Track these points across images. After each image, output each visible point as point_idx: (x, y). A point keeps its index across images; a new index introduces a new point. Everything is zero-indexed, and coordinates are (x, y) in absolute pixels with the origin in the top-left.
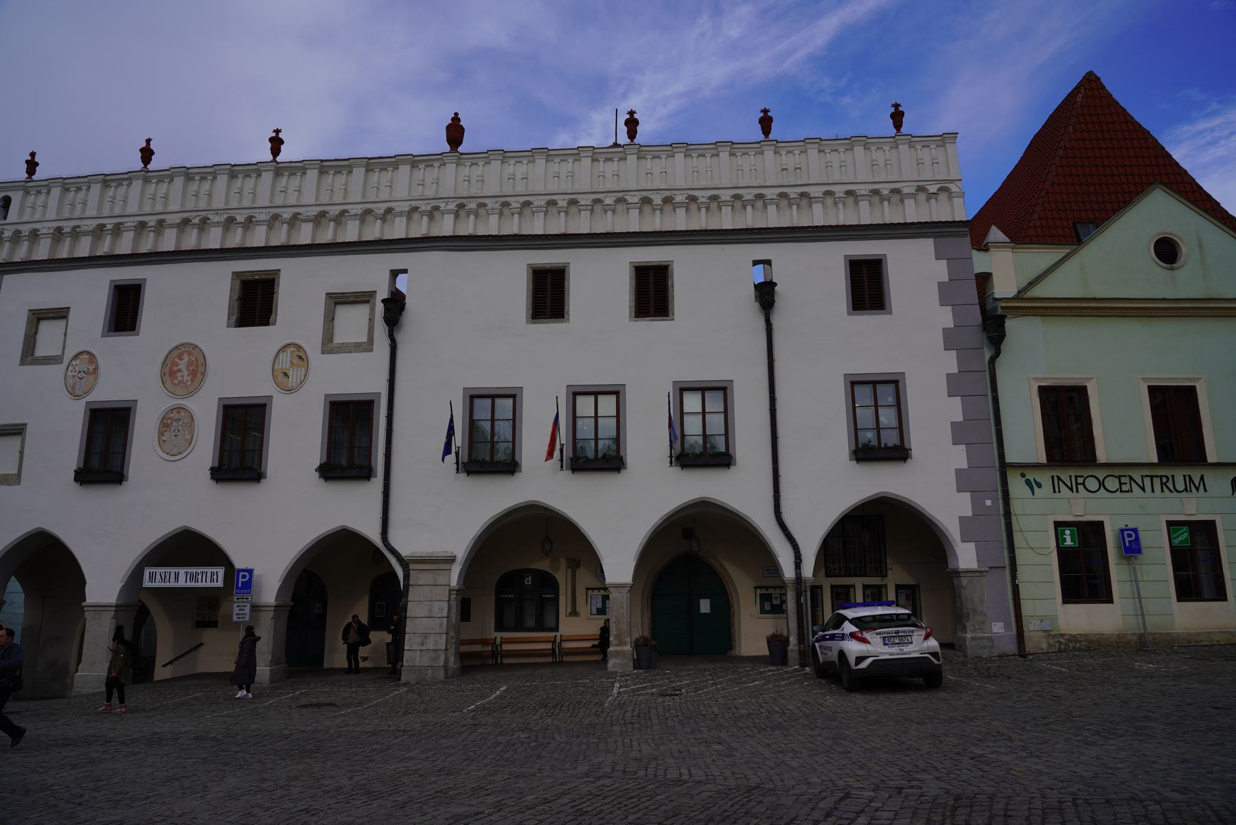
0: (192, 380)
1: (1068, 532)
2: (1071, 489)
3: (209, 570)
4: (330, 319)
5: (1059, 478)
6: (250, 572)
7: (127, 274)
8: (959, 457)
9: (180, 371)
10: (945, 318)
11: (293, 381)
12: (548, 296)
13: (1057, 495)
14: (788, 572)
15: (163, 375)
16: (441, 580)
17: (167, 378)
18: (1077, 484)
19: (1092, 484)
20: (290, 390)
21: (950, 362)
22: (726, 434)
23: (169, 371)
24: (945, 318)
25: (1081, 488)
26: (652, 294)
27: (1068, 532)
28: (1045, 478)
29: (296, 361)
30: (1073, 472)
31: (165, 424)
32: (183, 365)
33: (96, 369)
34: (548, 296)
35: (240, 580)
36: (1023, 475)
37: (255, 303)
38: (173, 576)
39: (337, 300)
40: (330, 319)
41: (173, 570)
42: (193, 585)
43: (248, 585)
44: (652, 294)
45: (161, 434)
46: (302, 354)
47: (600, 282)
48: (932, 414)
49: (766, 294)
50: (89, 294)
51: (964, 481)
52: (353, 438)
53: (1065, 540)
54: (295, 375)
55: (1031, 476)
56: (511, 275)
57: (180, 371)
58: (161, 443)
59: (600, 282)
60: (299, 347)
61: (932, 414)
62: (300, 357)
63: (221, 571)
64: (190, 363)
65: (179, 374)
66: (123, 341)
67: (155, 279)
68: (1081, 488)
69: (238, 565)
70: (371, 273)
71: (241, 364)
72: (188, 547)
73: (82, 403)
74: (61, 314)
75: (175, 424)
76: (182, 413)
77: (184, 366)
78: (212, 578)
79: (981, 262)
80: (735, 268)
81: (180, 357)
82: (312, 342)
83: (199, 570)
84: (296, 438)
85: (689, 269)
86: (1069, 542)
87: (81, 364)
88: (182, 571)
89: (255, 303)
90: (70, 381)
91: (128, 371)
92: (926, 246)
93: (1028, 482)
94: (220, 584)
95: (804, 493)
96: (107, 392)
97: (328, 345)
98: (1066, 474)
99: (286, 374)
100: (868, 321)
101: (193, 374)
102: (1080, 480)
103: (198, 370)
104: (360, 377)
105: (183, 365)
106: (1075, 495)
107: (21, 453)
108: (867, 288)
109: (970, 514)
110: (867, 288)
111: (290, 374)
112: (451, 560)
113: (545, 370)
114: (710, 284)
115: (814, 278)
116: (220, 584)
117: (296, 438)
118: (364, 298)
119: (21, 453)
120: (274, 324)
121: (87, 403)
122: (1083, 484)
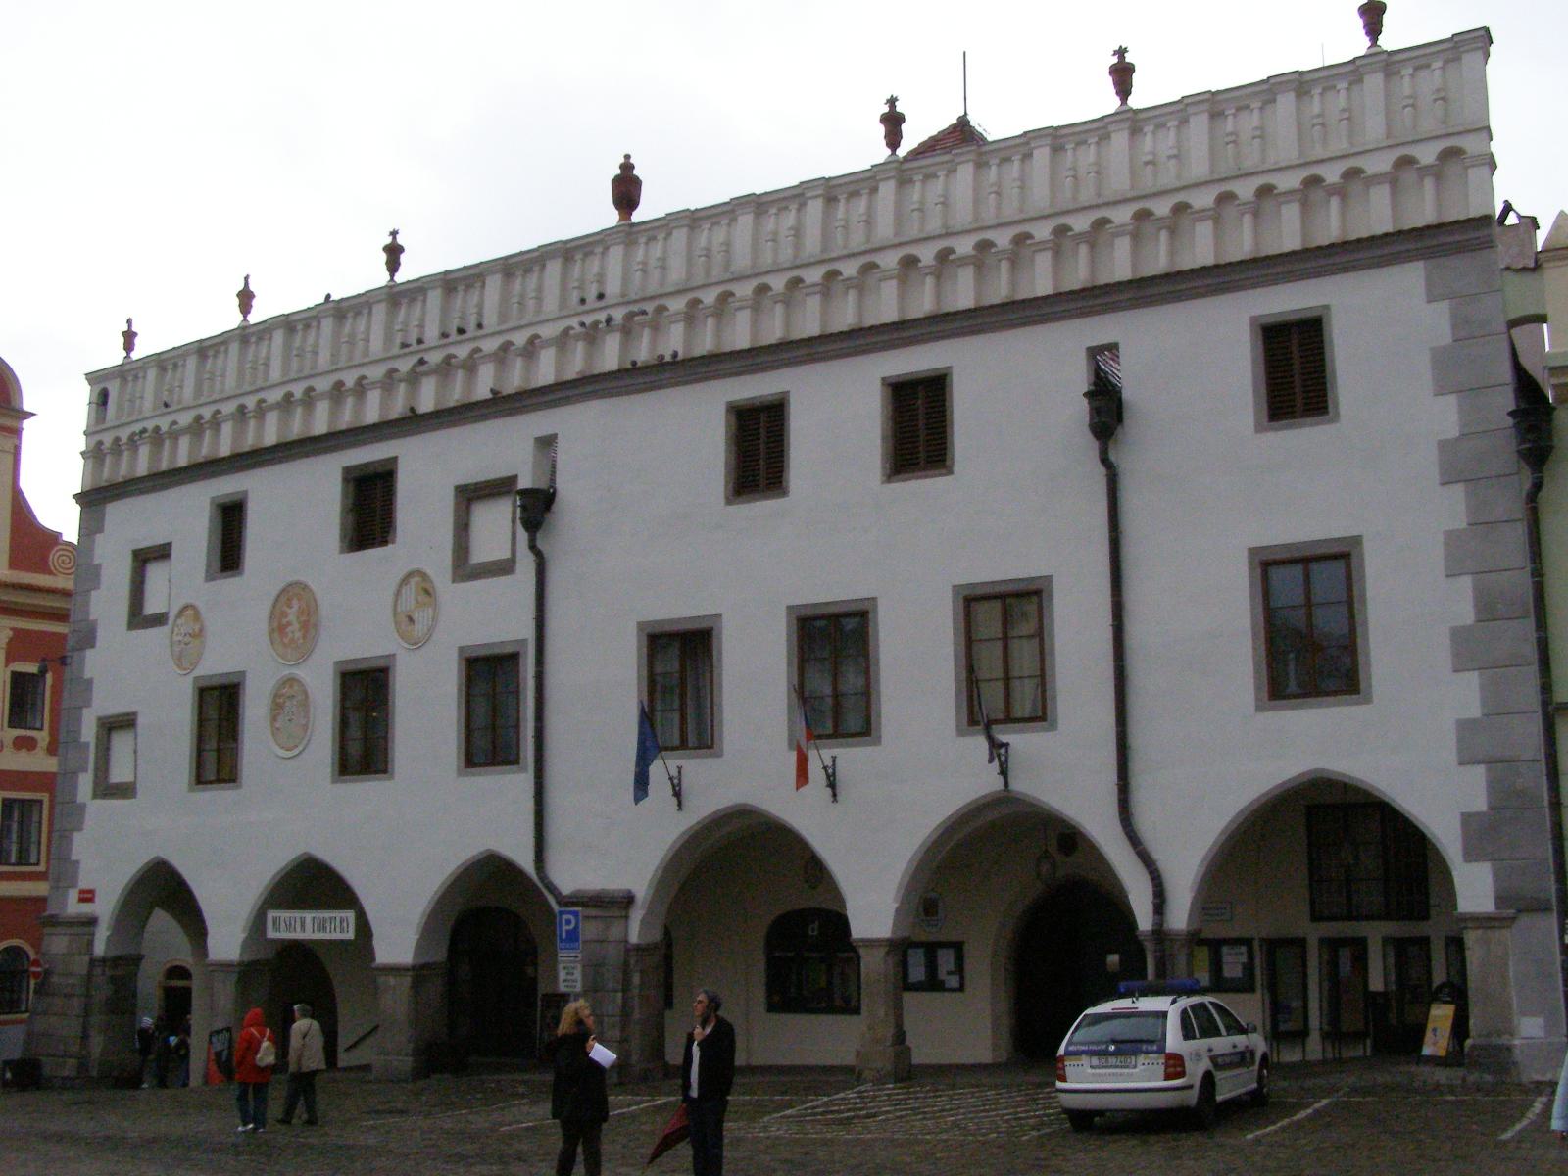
0: (304, 637)
4: (462, 528)
7: (226, 486)
8: (1465, 696)
9: (289, 624)
10: (1445, 417)
11: (419, 629)
12: (758, 454)
14: (1144, 921)
15: (271, 632)
16: (615, 932)
17: (276, 635)
21: (1451, 508)
22: (1042, 676)
23: (278, 628)
24: (1445, 417)
26: (919, 429)
29: (422, 597)
31: (277, 706)
34: (758, 454)
37: (370, 512)
38: (298, 920)
39: (470, 495)
40: (462, 528)
41: (297, 914)
44: (919, 429)
45: (274, 719)
46: (428, 586)
47: (836, 417)
48: (1415, 610)
49: (1107, 408)
51: (1473, 743)
54: (422, 617)
57: (289, 624)
58: (276, 731)
59: (836, 417)
61: (1415, 610)
62: (427, 592)
63: (350, 915)
65: (289, 629)
66: (230, 585)
70: (502, 449)
71: (360, 607)
72: (312, 883)
73: (190, 679)
74: (162, 552)
76: (296, 688)
77: (295, 615)
78: (337, 926)
80: (1047, 367)
82: (438, 562)
83: (327, 914)
84: (427, 712)
85: (986, 380)
87: (186, 625)
88: (309, 916)
89: (370, 512)
90: (177, 649)
92: (1408, 279)
94: (350, 935)
95: (1183, 777)
97: (464, 568)
99: (411, 620)
103: (310, 623)
104: (495, 615)
107: (135, 752)
108: (1295, 374)
110: (1295, 374)
111: (416, 617)
112: (627, 900)
113: (751, 579)
114: (1014, 396)
115: (1195, 365)
116: (350, 935)
117: (427, 712)
119: (135, 752)
120: (393, 542)
121: (196, 679)
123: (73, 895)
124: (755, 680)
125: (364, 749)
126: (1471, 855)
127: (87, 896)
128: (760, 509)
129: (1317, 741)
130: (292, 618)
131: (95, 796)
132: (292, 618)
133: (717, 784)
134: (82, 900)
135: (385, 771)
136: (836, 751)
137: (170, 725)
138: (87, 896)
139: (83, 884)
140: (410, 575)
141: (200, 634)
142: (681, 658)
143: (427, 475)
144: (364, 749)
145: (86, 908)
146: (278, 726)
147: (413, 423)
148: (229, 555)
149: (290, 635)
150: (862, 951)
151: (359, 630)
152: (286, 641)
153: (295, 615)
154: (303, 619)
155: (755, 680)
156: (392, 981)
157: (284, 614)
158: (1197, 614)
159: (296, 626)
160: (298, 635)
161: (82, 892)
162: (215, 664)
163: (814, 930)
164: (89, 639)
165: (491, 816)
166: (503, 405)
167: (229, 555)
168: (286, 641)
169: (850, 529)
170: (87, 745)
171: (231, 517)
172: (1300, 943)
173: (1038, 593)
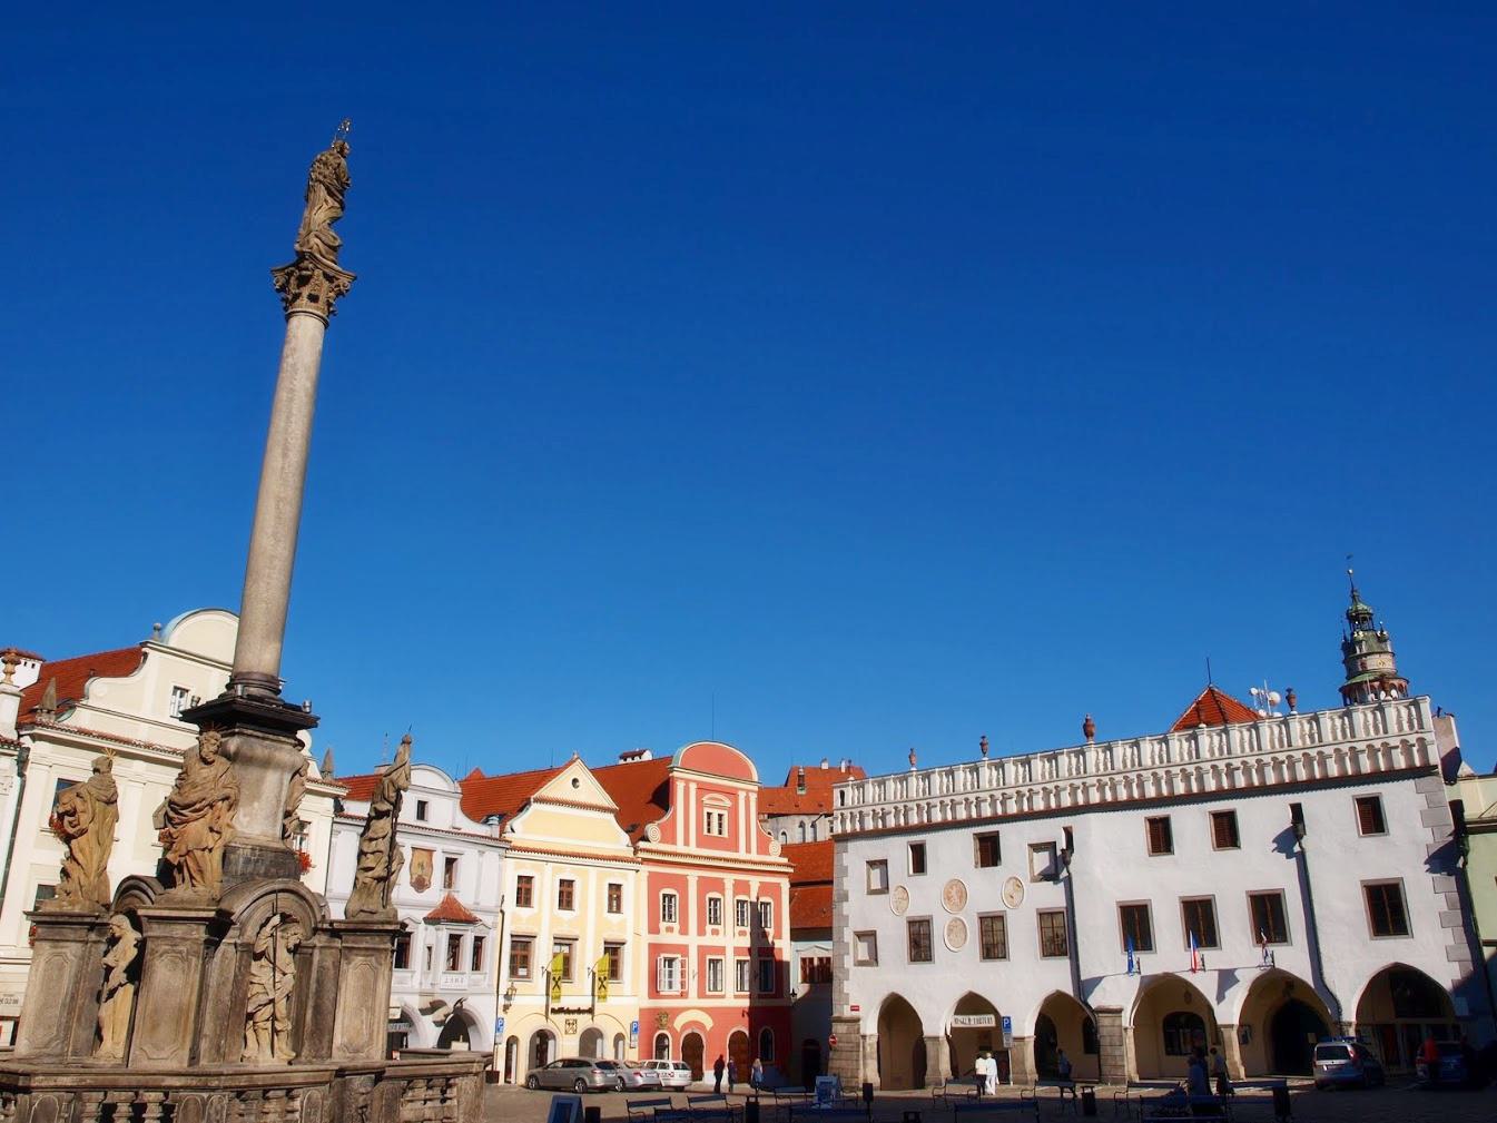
3: (987, 1016)
4: (1031, 861)
6: (1009, 1018)
11: (1016, 901)
12: (1161, 838)
20: (1016, 906)
26: (1227, 832)
32: (954, 892)
34: (1161, 838)
35: (1003, 1024)
37: (989, 852)
41: (966, 1017)
42: (979, 1025)
43: (1009, 1026)
44: (1227, 832)
47: (1192, 825)
50: (897, 851)
52: (1059, 937)
56: (1137, 821)
59: (1192, 825)
60: (1017, 879)
63: (993, 1017)
66: (920, 878)
67: (931, 840)
69: (1002, 1014)
70: (1052, 830)
71: (987, 889)
72: (972, 1003)
75: (957, 927)
79: (1450, 793)
81: (952, 888)
84: (1023, 935)
89: (989, 852)
91: (924, 897)
96: (917, 911)
100: (1373, 841)
101: (960, 897)
103: (963, 895)
104: (1053, 896)
105: (954, 892)
108: (1372, 818)
110: (1372, 818)
114: (1261, 819)
115: (1331, 812)
117: (1023, 935)
118: (1051, 846)
124: (1168, 925)
129: (1393, 951)
131: (855, 965)
133: (1152, 964)
135: (1004, 957)
139: (852, 1003)
140: (1011, 878)
145: (854, 1014)
147: (1007, 819)
148: (919, 866)
155: (1168, 925)
163: (1182, 1020)
164: (845, 898)
165: (1056, 977)
166: (1048, 813)
167: (919, 866)
169: (1196, 865)
171: (919, 852)
172: (1391, 1027)
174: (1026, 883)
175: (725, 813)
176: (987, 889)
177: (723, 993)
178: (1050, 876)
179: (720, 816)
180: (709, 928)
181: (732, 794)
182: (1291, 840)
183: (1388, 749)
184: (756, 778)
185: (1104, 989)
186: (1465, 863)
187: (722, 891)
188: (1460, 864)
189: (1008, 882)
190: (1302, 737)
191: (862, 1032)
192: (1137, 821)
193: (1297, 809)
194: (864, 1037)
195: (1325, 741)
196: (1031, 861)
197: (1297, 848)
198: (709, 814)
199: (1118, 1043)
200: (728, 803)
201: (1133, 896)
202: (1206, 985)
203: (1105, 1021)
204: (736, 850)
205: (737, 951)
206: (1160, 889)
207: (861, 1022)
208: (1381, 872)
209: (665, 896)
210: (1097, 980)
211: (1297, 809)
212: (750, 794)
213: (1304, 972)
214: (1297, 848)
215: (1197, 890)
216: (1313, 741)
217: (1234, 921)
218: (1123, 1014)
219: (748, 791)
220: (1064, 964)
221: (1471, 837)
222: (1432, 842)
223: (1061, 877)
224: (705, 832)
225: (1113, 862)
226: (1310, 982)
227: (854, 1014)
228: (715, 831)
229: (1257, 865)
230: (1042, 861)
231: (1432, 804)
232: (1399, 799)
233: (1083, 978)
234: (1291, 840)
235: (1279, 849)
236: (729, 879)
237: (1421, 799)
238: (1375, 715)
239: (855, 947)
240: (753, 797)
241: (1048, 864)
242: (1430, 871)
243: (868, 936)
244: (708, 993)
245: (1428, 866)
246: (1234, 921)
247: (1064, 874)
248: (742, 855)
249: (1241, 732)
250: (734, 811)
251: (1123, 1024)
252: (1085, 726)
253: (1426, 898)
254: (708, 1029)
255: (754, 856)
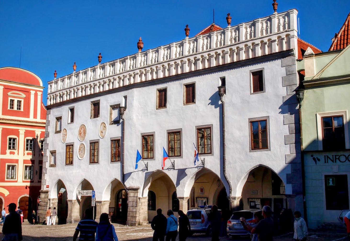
0: (84, 136)
1: (331, 180)
2: (333, 161)
4: (111, 114)
5: (328, 157)
9: (81, 133)
13: (326, 164)
18: (336, 159)
19: (343, 159)
25: (337, 160)
26: (191, 95)
27: (331, 180)
28: (322, 157)
29: (104, 128)
30: (334, 154)
33: (67, 134)
36: (312, 156)
44: (191, 95)
45: (79, 152)
53: (329, 183)
55: (316, 156)
56: (152, 92)
57: (81, 133)
64: (83, 131)
65: (81, 134)
68: (337, 160)
70: (117, 98)
71: (94, 130)
77: (83, 131)
86: (331, 184)
93: (314, 159)
98: (331, 155)
100: (258, 96)
102: (337, 157)
104: (115, 132)
106: (334, 164)
108: (259, 83)
109: (291, 173)
110: (259, 83)
117: (105, 151)
122: (339, 159)
123: (45, 186)
125: (94, 159)
126: (288, 182)
127: (48, 187)
128: (162, 110)
129: (261, 158)
130: (82, 132)
132: (82, 132)
133: (154, 166)
134: (47, 187)
136: (175, 159)
137: (61, 152)
138: (48, 187)
139: (47, 184)
141: (66, 135)
142: (147, 141)
143: (106, 102)
144: (94, 159)
146: (80, 153)
149: (82, 135)
150: (179, 200)
151: (93, 134)
152: (81, 136)
153: (83, 131)
154: (84, 132)
156: (98, 204)
157: (80, 131)
158: (239, 133)
159: (83, 133)
160: (83, 135)
161: (47, 186)
162: (69, 140)
168: (81, 136)
170: (48, 156)
172: (270, 200)
173: (210, 128)
174: (108, 125)
175: (23, 101)
176: (94, 130)
177: (16, 180)
178: (116, 122)
179: (19, 102)
180: (8, 151)
181: (27, 92)
182: (217, 99)
183: (271, 42)
184: (41, 85)
185: (133, 178)
186: (300, 106)
187: (17, 133)
188: (297, 108)
189: (101, 125)
190: (231, 40)
191: (49, 197)
192: (152, 92)
193: (223, 80)
194: (49, 200)
195: (241, 41)
196: (111, 114)
197: (220, 103)
198: (12, 101)
199: (135, 206)
200: (24, 96)
201: (147, 131)
202: (173, 175)
203: (131, 194)
204: (28, 117)
205: (25, 162)
206: (158, 125)
207: (49, 193)
208: (258, 115)
209: (10, 139)
210: (130, 174)
211: (223, 80)
212: (38, 92)
213: (217, 171)
214: (220, 103)
215: (174, 127)
216: (235, 41)
217: (189, 142)
218: (139, 191)
219: (36, 91)
220: (118, 165)
221: (305, 91)
222: (286, 95)
223: (120, 122)
224: (9, 108)
225: (143, 113)
226: (219, 175)
227: (47, 189)
228: (15, 108)
229: (204, 113)
230: (115, 114)
231: (289, 74)
232: (273, 71)
233: (125, 173)
234: (217, 99)
235: (212, 104)
236: (22, 130)
237: (283, 70)
238: (267, 23)
239: (50, 158)
240: (39, 94)
241: (117, 116)
242: (282, 112)
243: (53, 153)
244: (6, 180)
245: (280, 110)
246: (189, 142)
247: (121, 120)
248: (31, 119)
249: (203, 40)
250: (27, 100)
251: (139, 196)
252: (138, 43)
253: (279, 129)
254: (6, 195)
255: (39, 119)
